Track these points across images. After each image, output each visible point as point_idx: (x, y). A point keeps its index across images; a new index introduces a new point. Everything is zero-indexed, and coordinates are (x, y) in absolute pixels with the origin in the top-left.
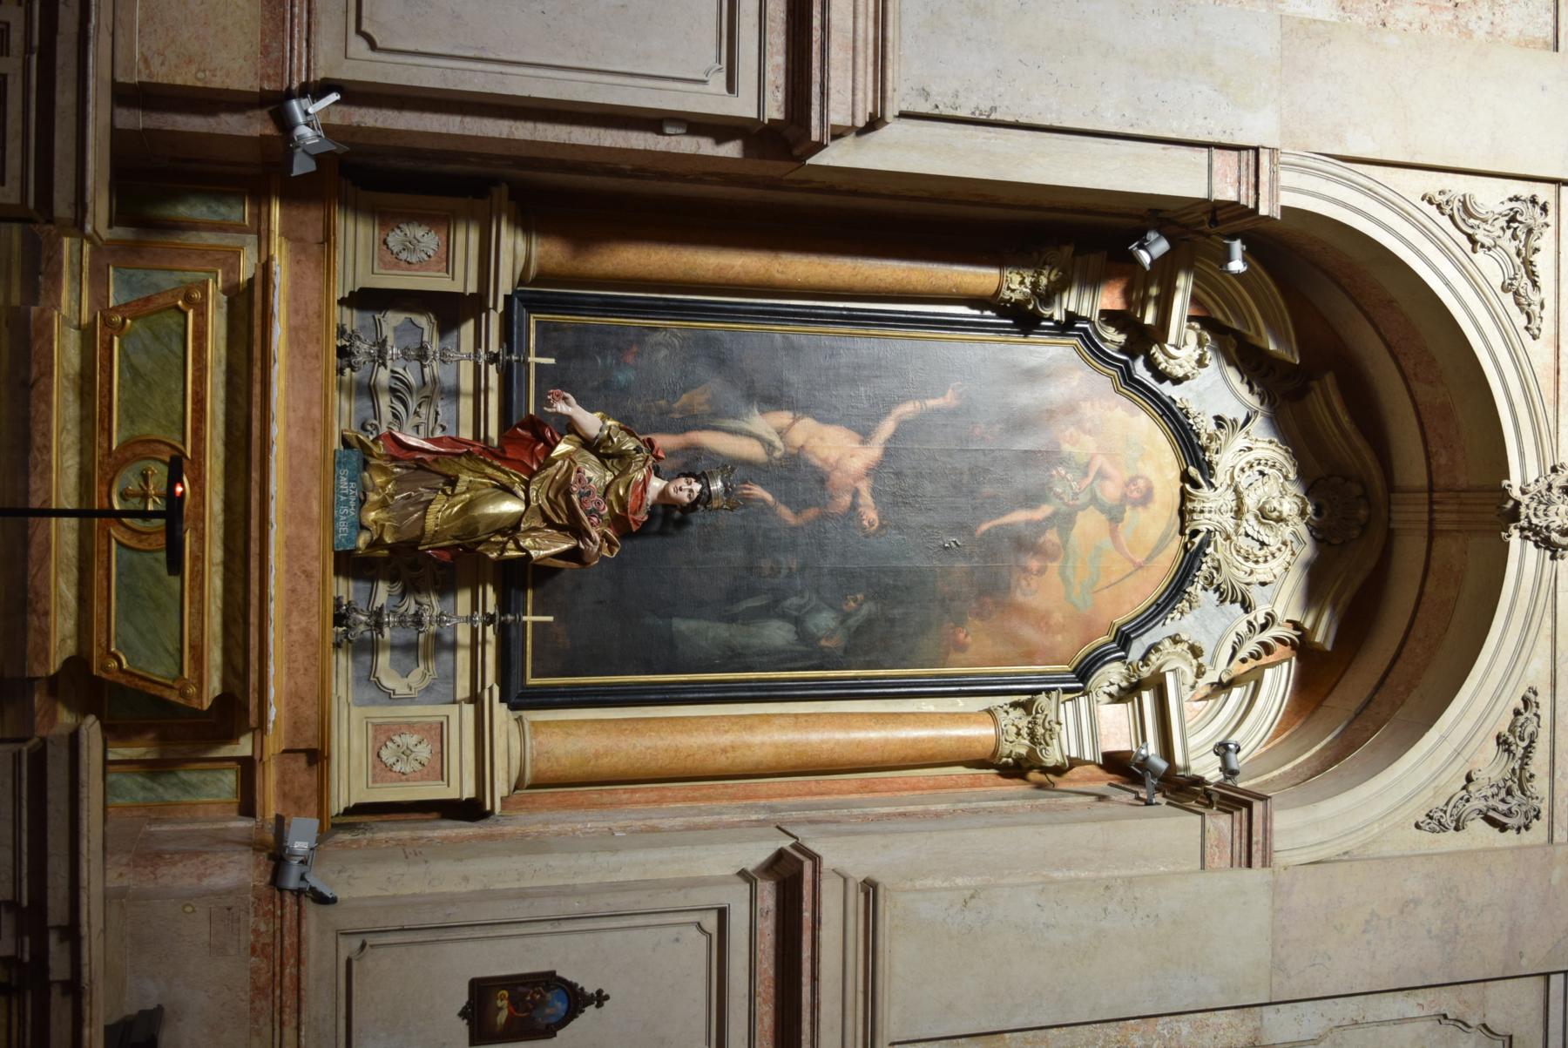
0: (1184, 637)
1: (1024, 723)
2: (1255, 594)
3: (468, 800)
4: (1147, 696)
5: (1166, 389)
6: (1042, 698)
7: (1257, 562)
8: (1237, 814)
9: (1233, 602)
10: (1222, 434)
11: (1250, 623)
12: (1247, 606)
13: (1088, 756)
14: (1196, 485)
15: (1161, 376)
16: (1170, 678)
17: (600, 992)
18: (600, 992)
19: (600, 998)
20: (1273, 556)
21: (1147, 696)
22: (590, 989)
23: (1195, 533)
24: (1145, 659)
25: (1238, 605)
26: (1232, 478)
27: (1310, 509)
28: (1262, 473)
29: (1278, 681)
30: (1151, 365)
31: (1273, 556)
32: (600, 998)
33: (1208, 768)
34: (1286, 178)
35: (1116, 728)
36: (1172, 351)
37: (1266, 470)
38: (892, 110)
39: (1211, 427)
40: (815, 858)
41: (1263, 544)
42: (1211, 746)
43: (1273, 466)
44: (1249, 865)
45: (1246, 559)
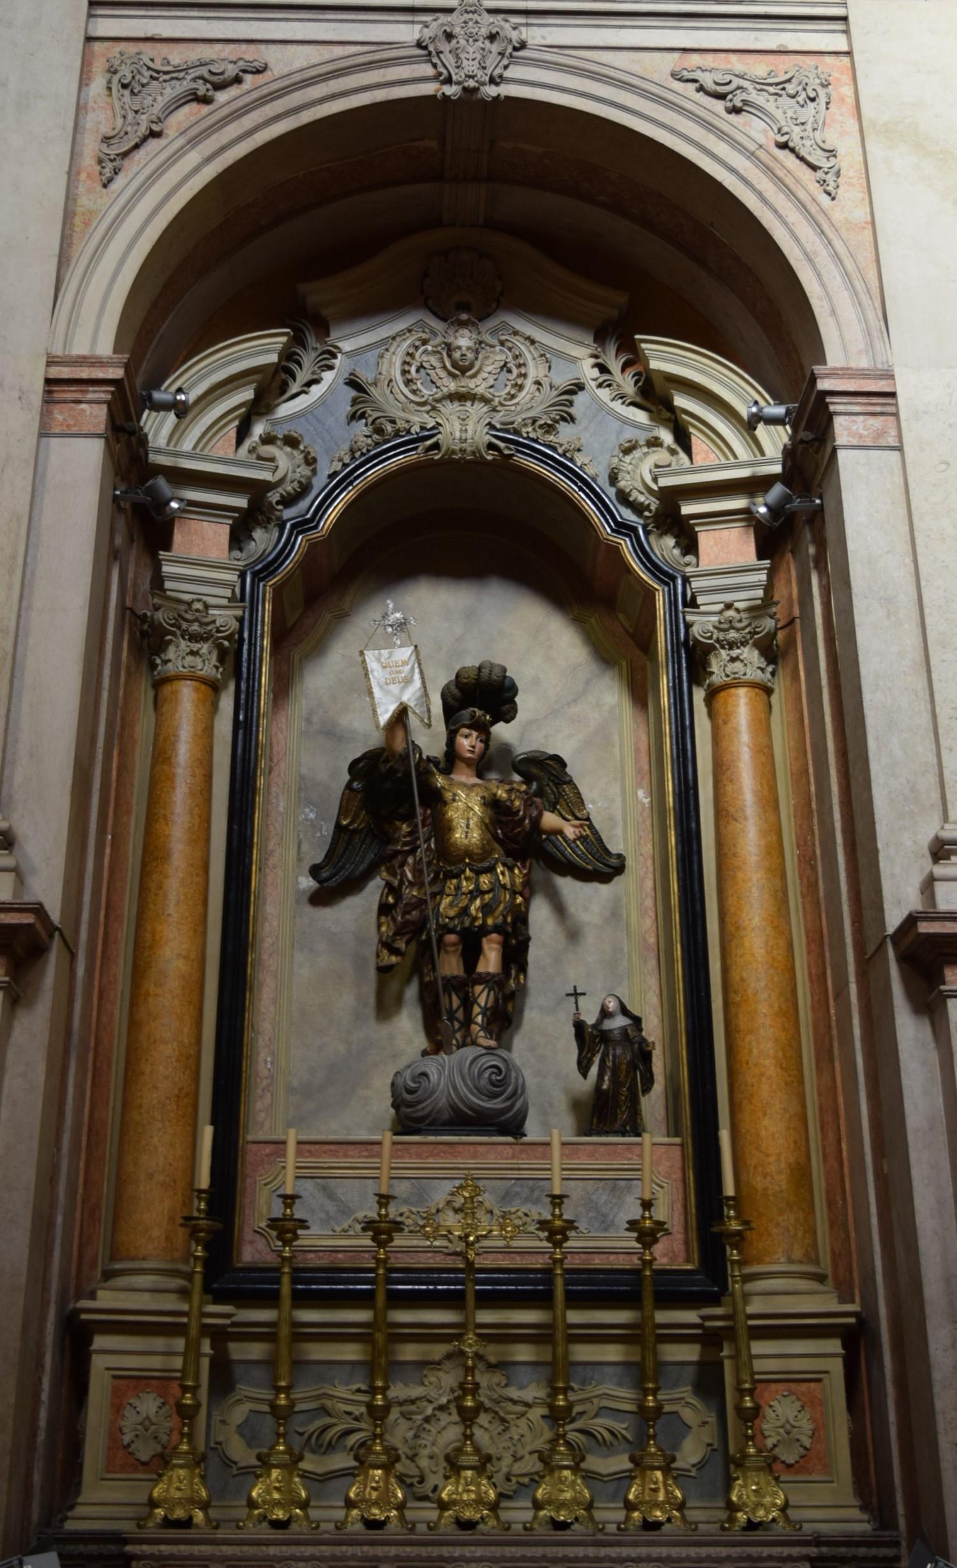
3: (844, 1347)
4: (687, 509)
7: (525, 376)
8: (832, 408)
9: (571, 403)
11: (600, 386)
13: (762, 577)
14: (436, 446)
16: (664, 482)
21: (687, 509)
24: (638, 509)
25: (574, 397)
27: (464, 317)
29: (666, 357)
30: (289, 501)
31: (516, 357)
33: (774, 441)
35: (727, 548)
36: (279, 475)
40: (912, 920)
44: (893, 395)
45: (521, 387)
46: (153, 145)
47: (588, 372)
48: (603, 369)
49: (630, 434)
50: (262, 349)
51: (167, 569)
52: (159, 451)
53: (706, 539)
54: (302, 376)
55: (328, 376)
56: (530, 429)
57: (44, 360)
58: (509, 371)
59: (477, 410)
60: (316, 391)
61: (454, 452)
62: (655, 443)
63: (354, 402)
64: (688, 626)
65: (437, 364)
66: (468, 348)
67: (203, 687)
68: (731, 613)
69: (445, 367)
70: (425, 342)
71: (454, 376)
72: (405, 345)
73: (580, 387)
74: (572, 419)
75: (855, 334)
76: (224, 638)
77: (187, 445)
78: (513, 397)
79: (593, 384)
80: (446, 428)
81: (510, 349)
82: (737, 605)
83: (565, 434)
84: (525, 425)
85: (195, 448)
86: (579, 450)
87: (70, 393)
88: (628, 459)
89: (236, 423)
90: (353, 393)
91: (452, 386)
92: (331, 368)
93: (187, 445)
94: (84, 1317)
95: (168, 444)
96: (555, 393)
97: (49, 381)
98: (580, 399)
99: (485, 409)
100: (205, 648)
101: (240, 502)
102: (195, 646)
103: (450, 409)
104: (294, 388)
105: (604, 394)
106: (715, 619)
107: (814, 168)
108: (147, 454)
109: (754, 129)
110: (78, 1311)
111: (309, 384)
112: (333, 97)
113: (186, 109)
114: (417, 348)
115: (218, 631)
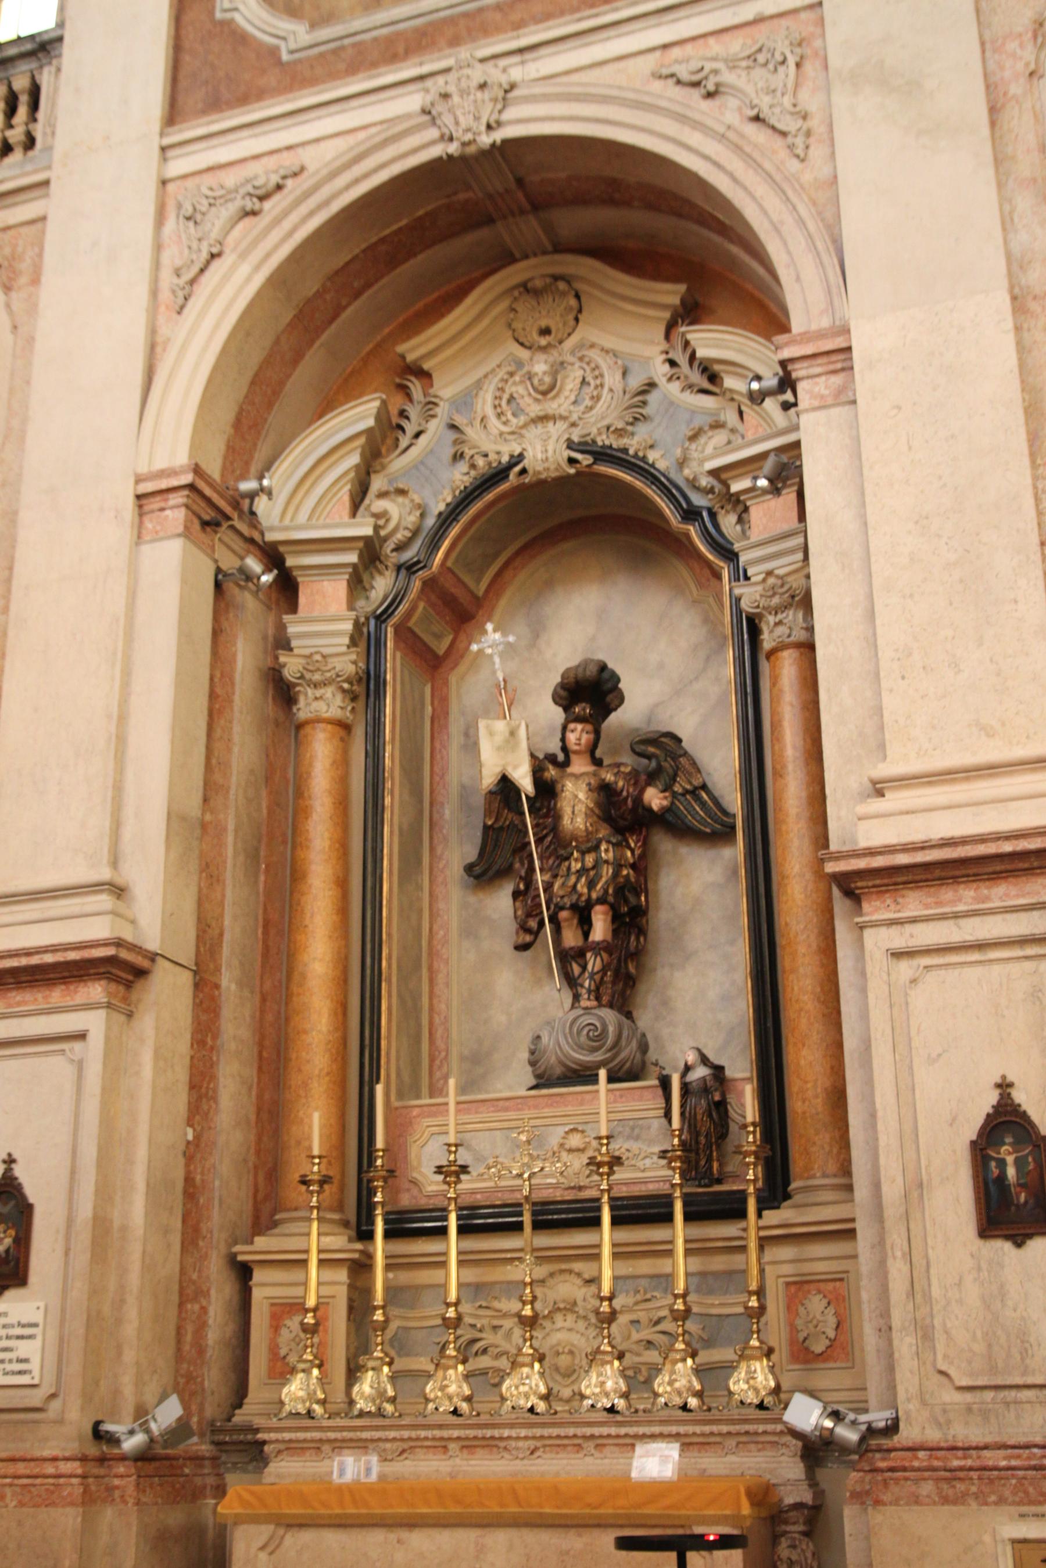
0: (678, 452)
1: (772, 619)
2: (635, 382)
5: (430, 521)
6: (744, 604)
7: (602, 385)
9: (645, 403)
10: (468, 452)
12: (652, 385)
14: (524, 471)
15: (416, 533)
17: (999, 1086)
18: (999, 1086)
19: (1004, 1086)
20: (594, 369)
22: (992, 1097)
23: (572, 461)
26: (513, 433)
28: (511, 399)
32: (1004, 1086)
34: (161, 463)
37: (506, 397)
38: (105, 874)
39: (463, 467)
41: (584, 382)
42: (756, 407)
43: (502, 390)
46: (216, 264)
47: (660, 370)
48: (672, 363)
49: (699, 421)
50: (360, 415)
51: (291, 630)
52: (272, 529)
53: (757, 513)
54: (410, 428)
55: (433, 426)
56: (604, 437)
57: (132, 480)
58: (589, 384)
59: (557, 431)
60: (423, 440)
61: (539, 473)
62: (717, 425)
63: (455, 442)
64: (738, 600)
65: (525, 393)
66: (545, 373)
67: (329, 727)
68: (771, 581)
69: (530, 394)
70: (511, 374)
71: (537, 400)
72: (496, 379)
73: (652, 385)
74: (645, 418)
75: (816, 295)
76: (344, 681)
77: (302, 517)
78: (591, 408)
79: (664, 380)
80: (529, 455)
81: (588, 364)
82: (777, 572)
83: (642, 434)
84: (600, 434)
85: (310, 518)
86: (652, 447)
87: (155, 503)
88: (693, 446)
89: (348, 487)
90: (452, 435)
91: (535, 410)
92: (434, 416)
93: (302, 517)
94: (240, 1258)
95: (281, 520)
96: (627, 396)
97: (139, 497)
98: (653, 398)
99: (565, 426)
100: (328, 692)
101: (353, 558)
102: (319, 693)
103: (534, 432)
104: (404, 442)
105: (675, 387)
106: (759, 588)
107: (784, 134)
108: (262, 534)
109: (729, 113)
110: (235, 1255)
111: (417, 435)
112: (357, 181)
113: (241, 225)
114: (506, 381)
115: (338, 676)
